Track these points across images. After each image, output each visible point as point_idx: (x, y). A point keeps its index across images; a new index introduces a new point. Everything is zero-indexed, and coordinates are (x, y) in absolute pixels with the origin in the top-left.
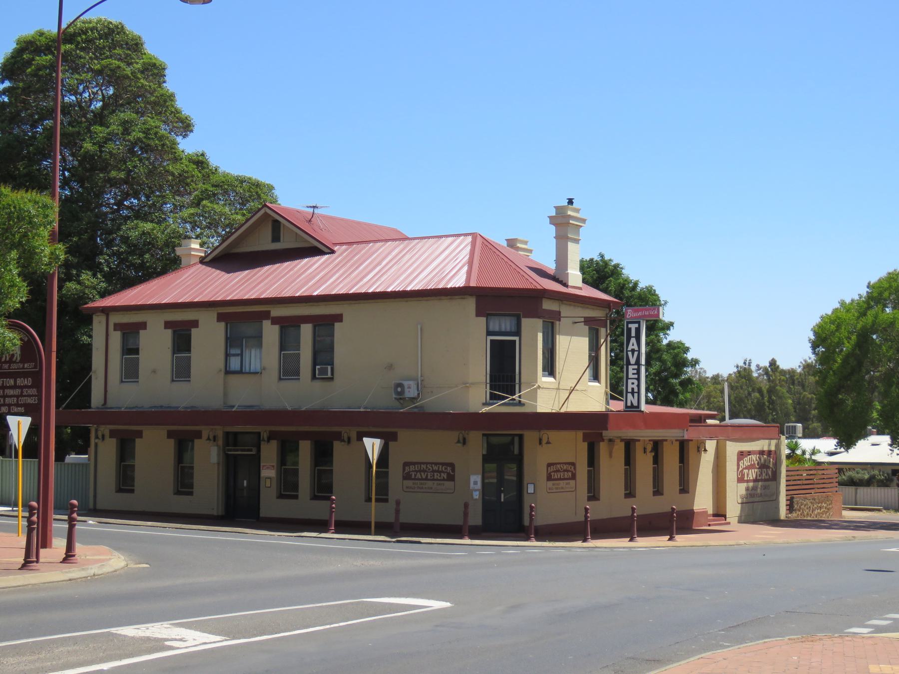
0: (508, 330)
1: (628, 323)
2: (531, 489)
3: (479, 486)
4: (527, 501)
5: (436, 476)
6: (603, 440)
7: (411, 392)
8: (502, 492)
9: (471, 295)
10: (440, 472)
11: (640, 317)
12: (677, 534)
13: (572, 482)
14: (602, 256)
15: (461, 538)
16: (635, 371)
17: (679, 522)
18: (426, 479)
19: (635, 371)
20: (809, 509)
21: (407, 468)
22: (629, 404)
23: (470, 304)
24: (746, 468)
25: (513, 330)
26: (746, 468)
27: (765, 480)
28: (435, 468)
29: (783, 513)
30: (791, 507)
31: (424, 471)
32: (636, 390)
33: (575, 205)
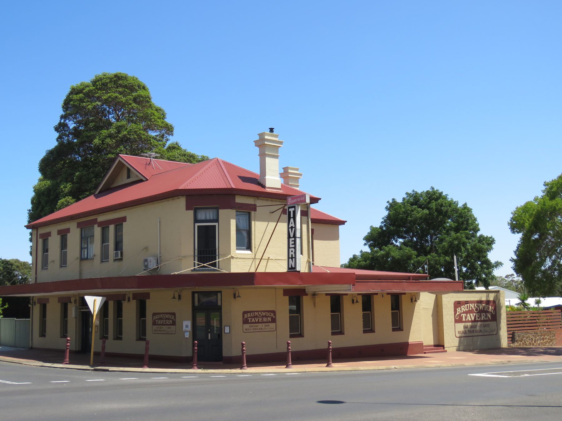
0: (212, 218)
1: (289, 208)
2: (227, 330)
3: (190, 328)
4: (224, 337)
5: (265, 320)
6: (307, 295)
7: (152, 265)
8: (209, 332)
9: (182, 196)
10: (169, 319)
11: (295, 203)
12: (333, 362)
13: (272, 325)
14: (433, 188)
15: (142, 366)
16: (293, 242)
17: (400, 351)
18: (258, 322)
19: (293, 242)
20: (527, 339)
21: (245, 315)
22: (290, 267)
23: (182, 202)
24: (464, 313)
25: (215, 218)
26: (464, 313)
27: (484, 321)
28: (264, 314)
29: (504, 343)
30: (512, 338)
31: (257, 317)
32: (294, 256)
33: (274, 133)
